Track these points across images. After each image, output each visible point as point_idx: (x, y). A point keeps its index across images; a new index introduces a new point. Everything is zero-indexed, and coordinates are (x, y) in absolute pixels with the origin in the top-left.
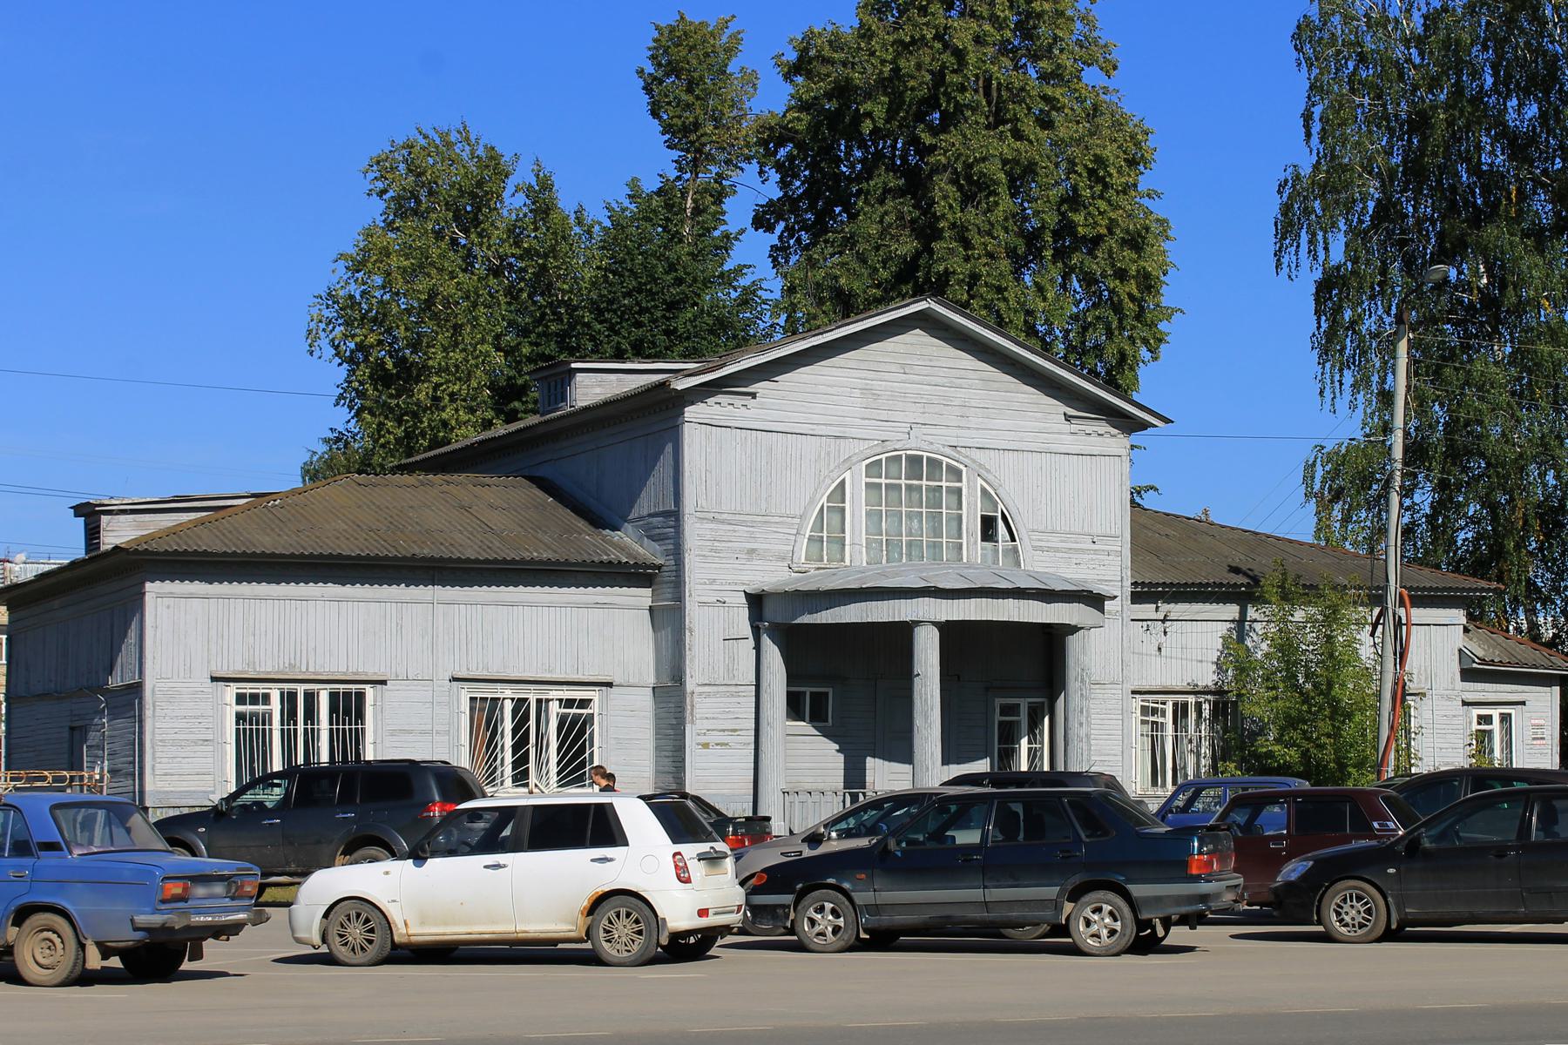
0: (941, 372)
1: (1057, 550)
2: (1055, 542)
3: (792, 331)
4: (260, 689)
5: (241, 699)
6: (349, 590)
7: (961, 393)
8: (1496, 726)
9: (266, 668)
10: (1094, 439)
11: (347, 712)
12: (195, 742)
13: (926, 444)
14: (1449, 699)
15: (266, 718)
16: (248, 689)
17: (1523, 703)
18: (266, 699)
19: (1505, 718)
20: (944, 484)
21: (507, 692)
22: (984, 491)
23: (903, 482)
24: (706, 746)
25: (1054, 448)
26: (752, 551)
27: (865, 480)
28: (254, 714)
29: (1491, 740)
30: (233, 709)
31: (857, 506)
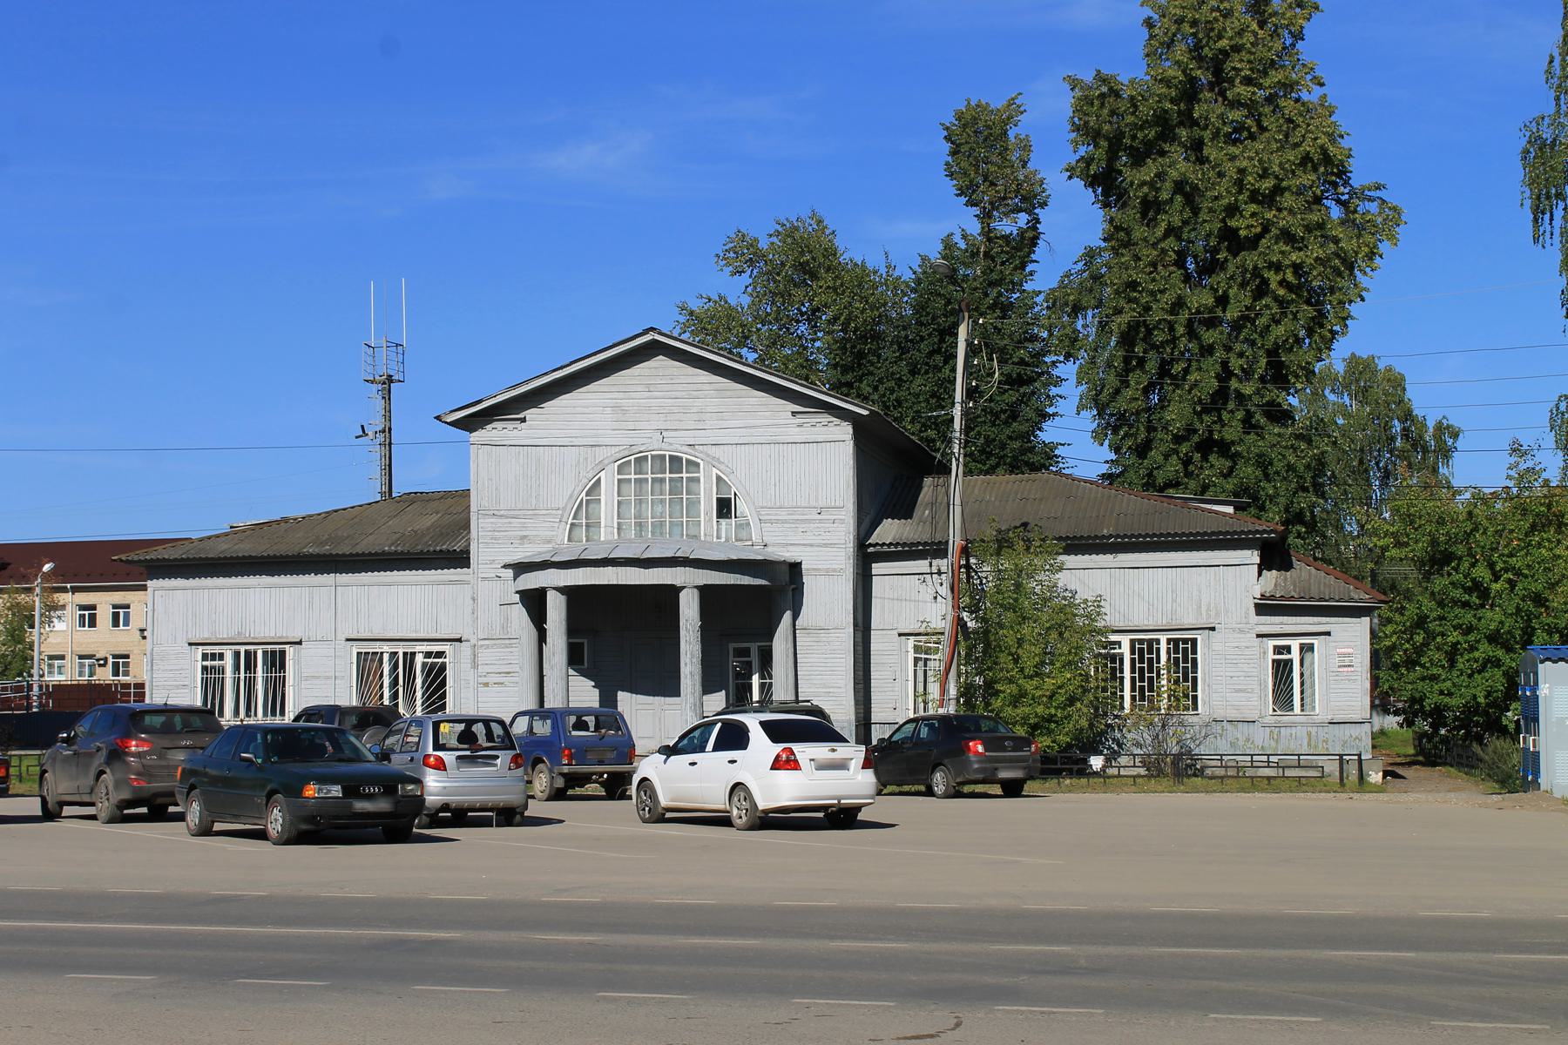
0: (680, 387)
1: (785, 522)
2: (783, 515)
3: (761, 363)
4: (217, 650)
5: (205, 657)
6: (276, 580)
7: (699, 402)
8: (1295, 655)
9: (223, 635)
10: (819, 429)
11: (273, 664)
12: (177, 687)
13: (675, 445)
14: (1241, 631)
15: (222, 670)
16: (209, 650)
17: (1328, 634)
18: (221, 657)
19: (1307, 649)
20: (684, 475)
21: (386, 648)
22: (719, 478)
23: (649, 476)
24: (486, 685)
25: (780, 439)
26: (523, 538)
27: (617, 477)
28: (213, 667)
29: (1291, 670)
30: (1271, 656)
31: (608, 494)
